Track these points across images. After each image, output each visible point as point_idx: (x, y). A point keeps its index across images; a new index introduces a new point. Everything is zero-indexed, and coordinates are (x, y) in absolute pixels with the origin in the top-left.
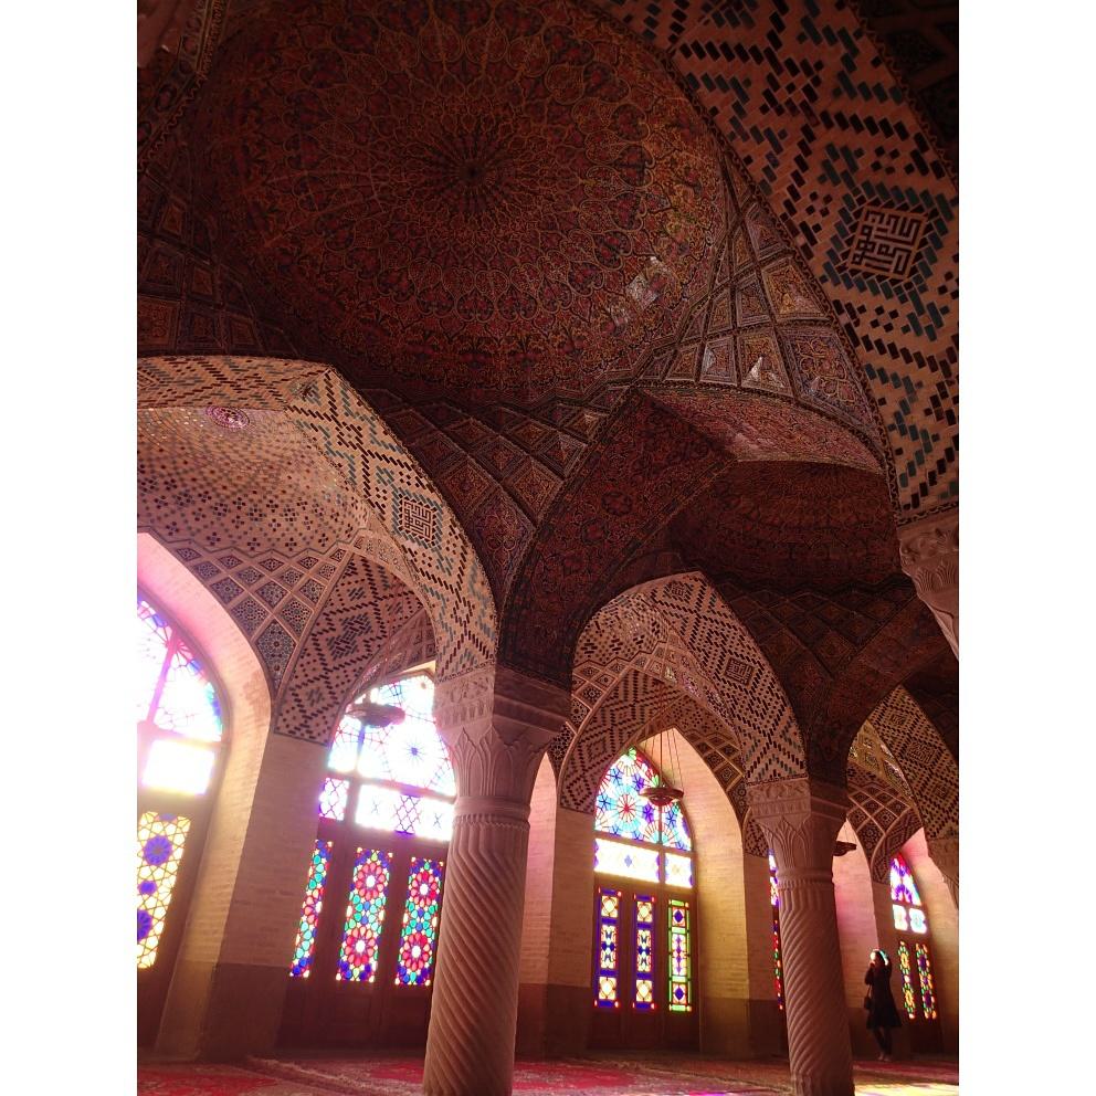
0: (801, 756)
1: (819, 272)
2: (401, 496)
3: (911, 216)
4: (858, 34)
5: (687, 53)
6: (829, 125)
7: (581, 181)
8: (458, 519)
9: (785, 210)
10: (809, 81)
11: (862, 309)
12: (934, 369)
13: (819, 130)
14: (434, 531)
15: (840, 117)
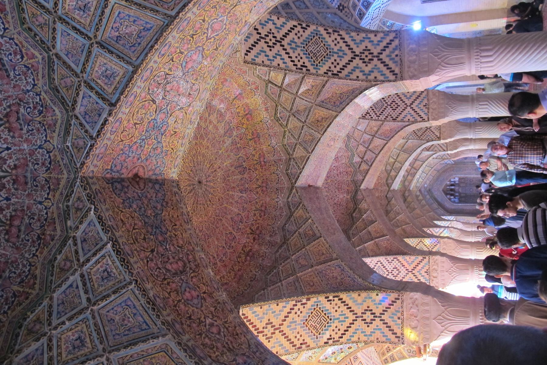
0: (420, 258)
1: (314, 71)
2: (304, 323)
3: (314, 40)
4: (271, 17)
5: (246, 54)
6: (283, 40)
7: (220, 152)
8: (326, 293)
9: (295, 67)
10: (272, 35)
11: (330, 67)
12: (355, 59)
13: (283, 43)
14: (325, 314)
15: (283, 36)
